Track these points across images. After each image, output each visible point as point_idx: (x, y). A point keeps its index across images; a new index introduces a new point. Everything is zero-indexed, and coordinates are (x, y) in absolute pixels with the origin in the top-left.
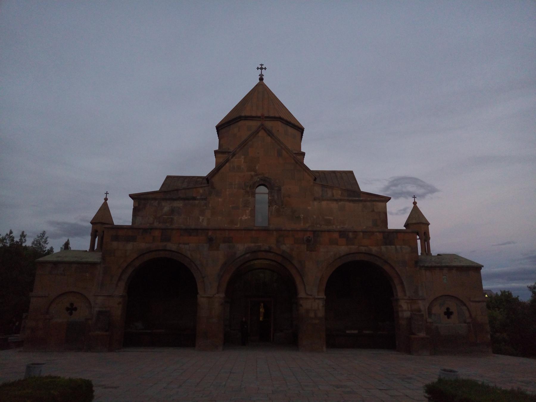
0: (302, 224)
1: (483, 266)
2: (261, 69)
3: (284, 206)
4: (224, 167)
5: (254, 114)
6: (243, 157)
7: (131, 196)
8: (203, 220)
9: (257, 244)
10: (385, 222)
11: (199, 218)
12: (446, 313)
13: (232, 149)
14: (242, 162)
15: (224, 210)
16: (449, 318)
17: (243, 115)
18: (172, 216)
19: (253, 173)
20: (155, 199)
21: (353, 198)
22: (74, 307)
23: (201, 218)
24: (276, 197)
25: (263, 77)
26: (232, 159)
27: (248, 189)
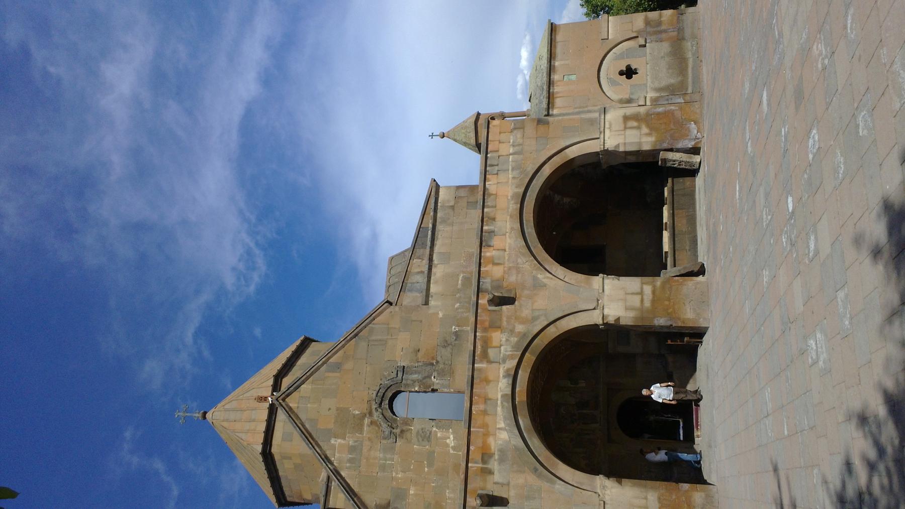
3: (434, 361)
4: (349, 482)
5: (262, 427)
6: (333, 441)
9: (499, 402)
10: (472, 189)
13: (323, 475)
14: (343, 442)
15: (434, 485)
17: (259, 448)
21: (428, 239)
24: (415, 376)
26: (335, 464)
27: (397, 431)
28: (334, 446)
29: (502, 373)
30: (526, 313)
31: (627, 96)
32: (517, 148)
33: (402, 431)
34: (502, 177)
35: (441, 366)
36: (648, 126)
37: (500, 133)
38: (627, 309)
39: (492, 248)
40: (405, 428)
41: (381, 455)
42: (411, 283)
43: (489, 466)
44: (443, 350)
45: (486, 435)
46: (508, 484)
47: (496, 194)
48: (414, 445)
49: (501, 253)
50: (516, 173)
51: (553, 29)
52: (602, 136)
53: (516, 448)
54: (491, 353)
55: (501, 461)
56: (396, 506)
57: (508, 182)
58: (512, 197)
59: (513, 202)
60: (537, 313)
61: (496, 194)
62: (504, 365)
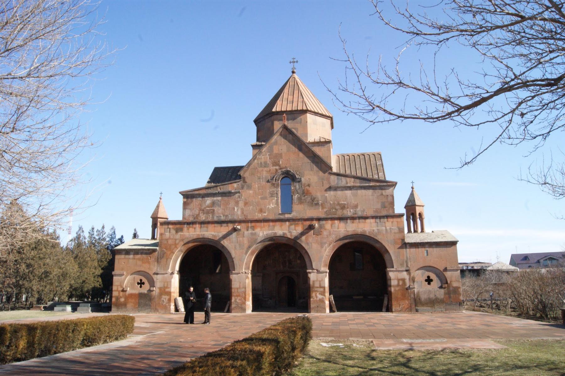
0: (320, 210)
1: (458, 241)
2: (294, 62)
7: (180, 193)
8: (238, 210)
9: (273, 231)
10: (392, 204)
11: (234, 209)
12: (426, 281)
16: (429, 284)
17: (274, 110)
18: (213, 208)
19: (277, 167)
20: (199, 196)
22: (142, 282)
23: (235, 208)
24: (297, 187)
25: (295, 70)
28: (266, 155)
29: (285, 231)
30: (310, 240)
31: (416, 280)
32: (389, 231)
33: (274, 184)
34: (374, 224)
35: (303, 198)
36: (399, 290)
37: (397, 222)
38: (314, 281)
39: (339, 223)
40: (275, 185)
41: (264, 176)
42: (341, 179)
43: (250, 229)
44: (309, 198)
45: (261, 228)
46: (244, 237)
47: (365, 222)
48: (269, 190)
49: (337, 228)
50: (376, 231)
51: (453, 244)
52: (394, 269)
53: (256, 239)
54: (293, 227)
55: (252, 234)
56: (245, 185)
57: (371, 227)
58: (364, 230)
59: (361, 230)
60: (310, 245)
61: (365, 222)
62: (287, 231)
